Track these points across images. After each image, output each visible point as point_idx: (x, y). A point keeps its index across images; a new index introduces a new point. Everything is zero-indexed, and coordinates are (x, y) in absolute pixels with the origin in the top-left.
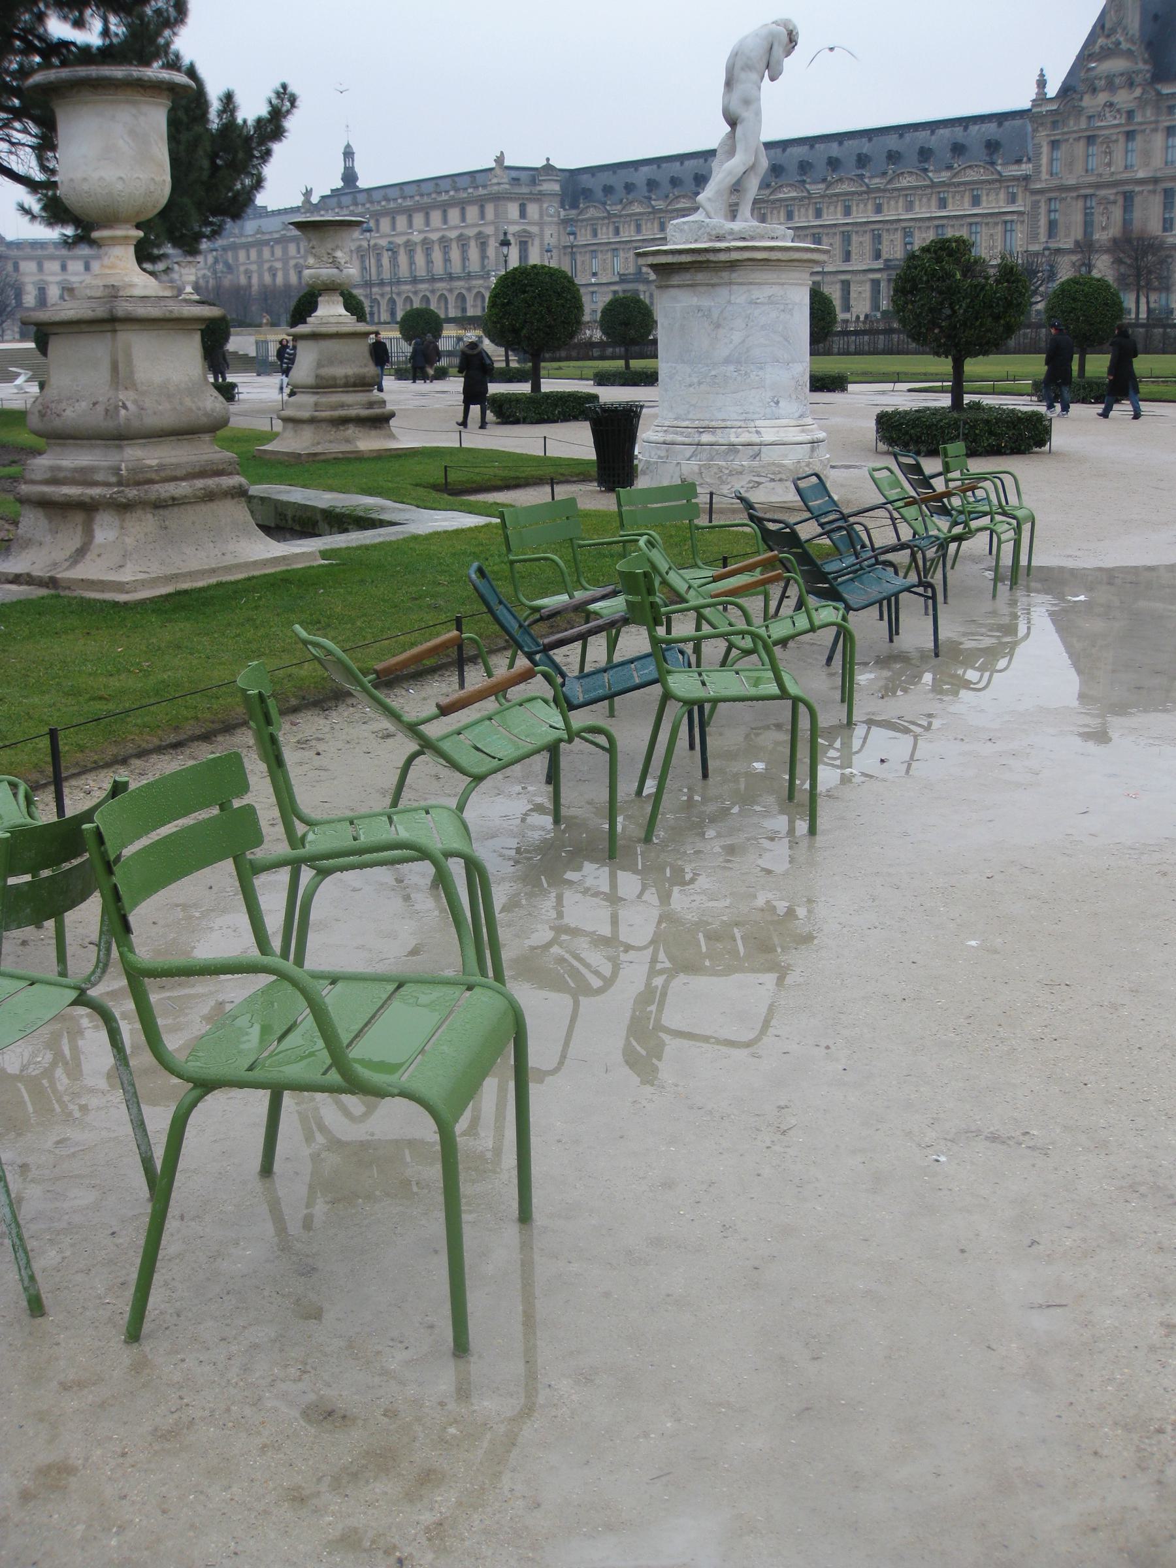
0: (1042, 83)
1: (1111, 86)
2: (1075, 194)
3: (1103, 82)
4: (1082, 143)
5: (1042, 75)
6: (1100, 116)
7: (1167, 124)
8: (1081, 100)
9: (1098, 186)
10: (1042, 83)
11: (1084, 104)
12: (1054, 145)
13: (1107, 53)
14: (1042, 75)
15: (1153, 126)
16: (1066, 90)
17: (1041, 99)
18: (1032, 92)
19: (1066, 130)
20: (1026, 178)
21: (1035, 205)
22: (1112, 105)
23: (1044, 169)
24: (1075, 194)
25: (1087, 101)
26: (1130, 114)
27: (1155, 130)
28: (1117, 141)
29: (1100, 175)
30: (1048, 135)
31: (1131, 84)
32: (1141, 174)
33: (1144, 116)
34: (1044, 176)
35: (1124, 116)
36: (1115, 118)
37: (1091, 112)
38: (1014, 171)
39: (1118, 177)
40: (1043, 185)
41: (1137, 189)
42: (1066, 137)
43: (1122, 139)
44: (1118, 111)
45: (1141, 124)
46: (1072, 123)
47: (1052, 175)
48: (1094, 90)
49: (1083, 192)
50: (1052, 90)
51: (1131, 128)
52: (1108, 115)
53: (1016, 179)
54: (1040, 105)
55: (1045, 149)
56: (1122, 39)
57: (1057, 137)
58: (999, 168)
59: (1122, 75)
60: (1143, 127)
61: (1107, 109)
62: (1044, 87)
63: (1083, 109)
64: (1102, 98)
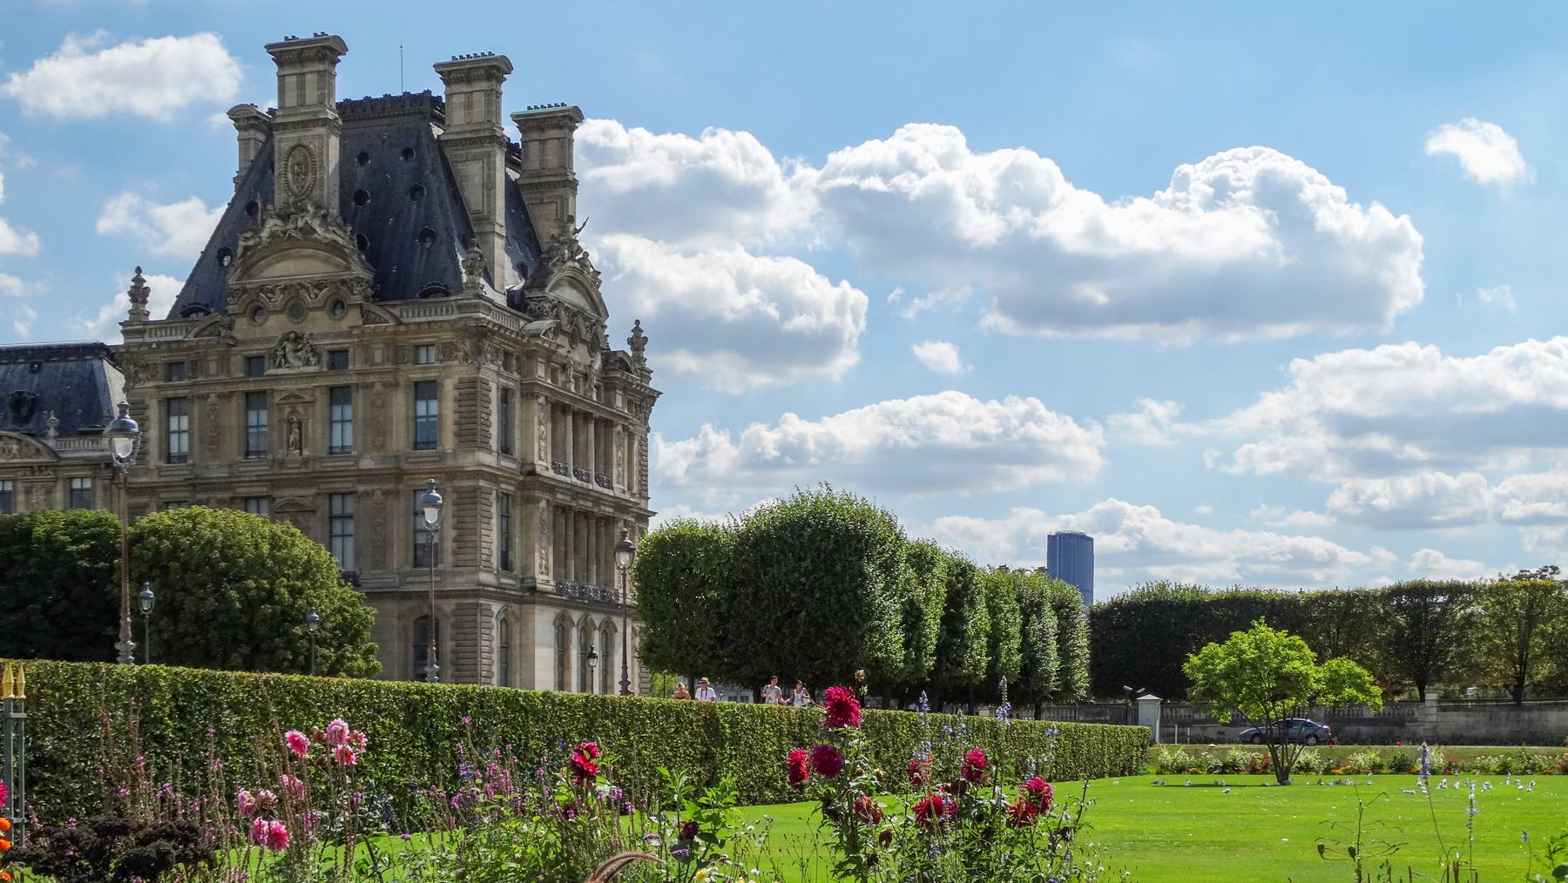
0: (139, 293)
2: (226, 495)
3: (279, 299)
4: (235, 404)
5: (139, 281)
6: (278, 358)
8: (230, 327)
9: (276, 483)
10: (139, 293)
11: (239, 335)
13: (282, 245)
14: (139, 281)
15: (389, 378)
16: (185, 309)
19: (201, 379)
22: (298, 338)
23: (153, 448)
24: (226, 495)
25: (242, 328)
26: (338, 359)
27: (395, 385)
28: (313, 403)
29: (282, 463)
30: (157, 387)
31: (337, 305)
32: (367, 464)
33: (368, 360)
34: (154, 460)
35: (325, 358)
36: (308, 363)
38: (79, 449)
39: (318, 467)
40: (155, 478)
41: (361, 488)
42: (202, 392)
43: (322, 399)
44: (313, 350)
45: (360, 373)
46: (213, 367)
47: (169, 458)
49: (243, 491)
50: (160, 307)
51: (342, 381)
52: (290, 356)
54: (141, 333)
56: (316, 224)
57: (181, 392)
58: (51, 443)
59: (319, 286)
60: (371, 379)
61: (289, 346)
62: (145, 302)
63: (237, 342)
64: (276, 325)
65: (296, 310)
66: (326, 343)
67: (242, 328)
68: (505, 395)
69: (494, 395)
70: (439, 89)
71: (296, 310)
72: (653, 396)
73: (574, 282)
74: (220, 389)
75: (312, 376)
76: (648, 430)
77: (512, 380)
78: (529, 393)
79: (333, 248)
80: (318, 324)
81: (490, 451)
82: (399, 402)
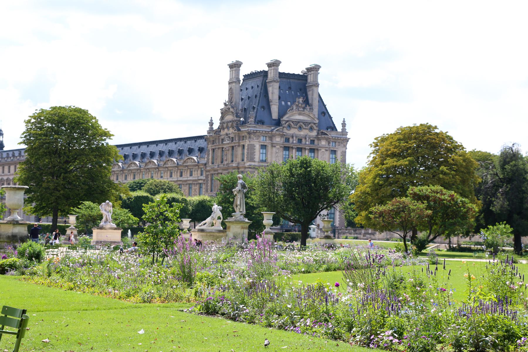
0: (211, 124)
1: (228, 128)
7: (242, 144)
8: (220, 132)
10: (211, 124)
17: (211, 130)
18: (208, 127)
21: (207, 177)
22: (227, 135)
24: (217, 172)
27: (239, 146)
28: (228, 150)
32: (234, 165)
34: (210, 164)
48: (224, 129)
50: (216, 127)
53: (202, 164)
55: (210, 152)
64: (226, 130)
68: (263, 147)
69: (257, 147)
70: (266, 69)
72: (347, 140)
73: (300, 114)
74: (217, 147)
75: (228, 144)
76: (346, 148)
81: (255, 162)
82: (239, 150)
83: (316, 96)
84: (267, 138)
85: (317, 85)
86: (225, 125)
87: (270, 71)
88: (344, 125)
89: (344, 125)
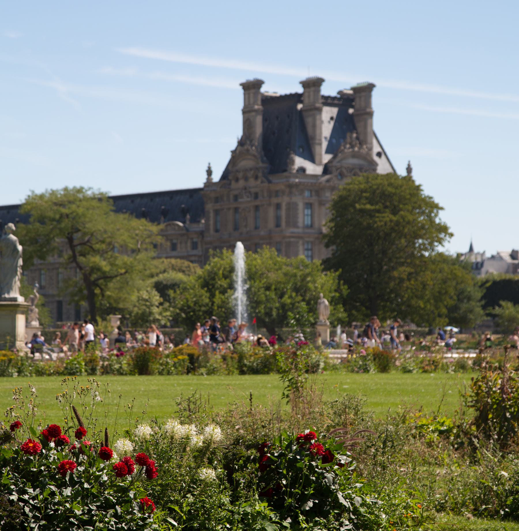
0: (209, 172)
8: (230, 184)
10: (209, 172)
12: (217, 212)
16: (225, 176)
20: (202, 234)
32: (262, 233)
34: (212, 231)
37: (236, 192)
58: (187, 226)
64: (242, 183)
65: (246, 179)
66: (253, 190)
67: (234, 185)
69: (301, 206)
71: (246, 179)
77: (314, 199)
78: (321, 203)
79: (254, 156)
80: (252, 182)
81: (298, 227)
82: (271, 212)
83: (369, 129)
84: (313, 193)
85: (370, 114)
86: (240, 175)
87: (306, 94)
88: (409, 170)
89: (409, 170)
